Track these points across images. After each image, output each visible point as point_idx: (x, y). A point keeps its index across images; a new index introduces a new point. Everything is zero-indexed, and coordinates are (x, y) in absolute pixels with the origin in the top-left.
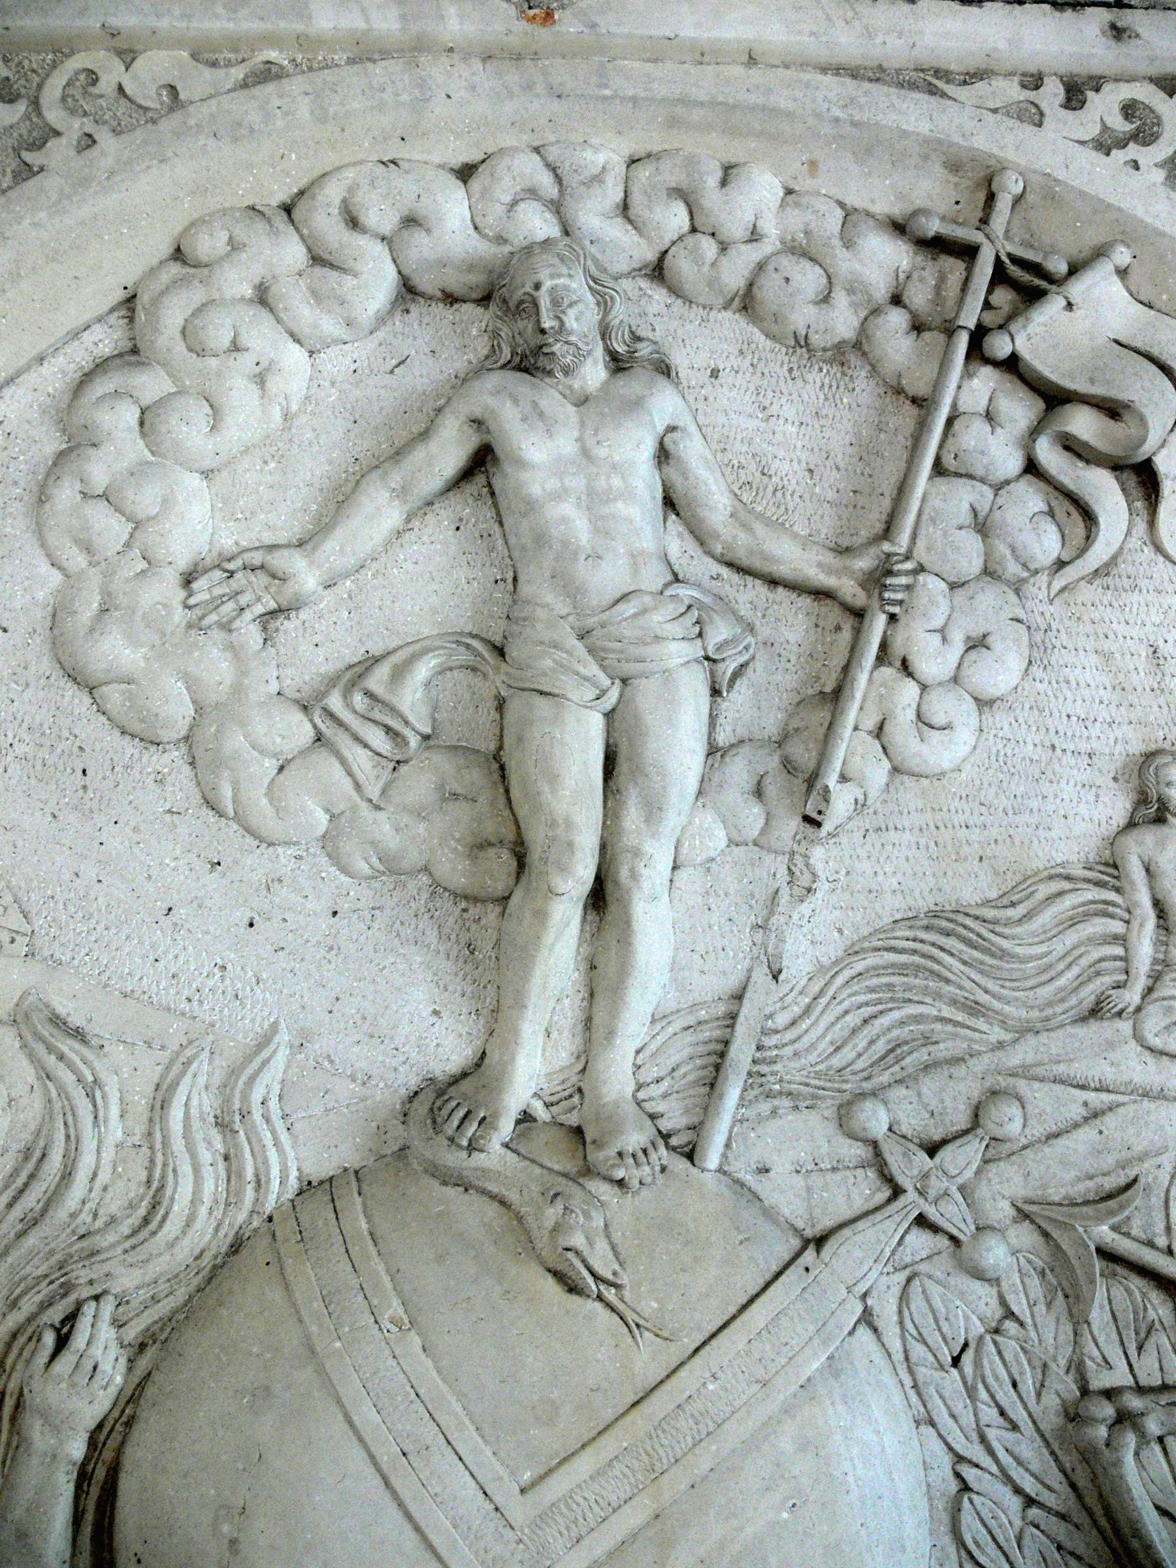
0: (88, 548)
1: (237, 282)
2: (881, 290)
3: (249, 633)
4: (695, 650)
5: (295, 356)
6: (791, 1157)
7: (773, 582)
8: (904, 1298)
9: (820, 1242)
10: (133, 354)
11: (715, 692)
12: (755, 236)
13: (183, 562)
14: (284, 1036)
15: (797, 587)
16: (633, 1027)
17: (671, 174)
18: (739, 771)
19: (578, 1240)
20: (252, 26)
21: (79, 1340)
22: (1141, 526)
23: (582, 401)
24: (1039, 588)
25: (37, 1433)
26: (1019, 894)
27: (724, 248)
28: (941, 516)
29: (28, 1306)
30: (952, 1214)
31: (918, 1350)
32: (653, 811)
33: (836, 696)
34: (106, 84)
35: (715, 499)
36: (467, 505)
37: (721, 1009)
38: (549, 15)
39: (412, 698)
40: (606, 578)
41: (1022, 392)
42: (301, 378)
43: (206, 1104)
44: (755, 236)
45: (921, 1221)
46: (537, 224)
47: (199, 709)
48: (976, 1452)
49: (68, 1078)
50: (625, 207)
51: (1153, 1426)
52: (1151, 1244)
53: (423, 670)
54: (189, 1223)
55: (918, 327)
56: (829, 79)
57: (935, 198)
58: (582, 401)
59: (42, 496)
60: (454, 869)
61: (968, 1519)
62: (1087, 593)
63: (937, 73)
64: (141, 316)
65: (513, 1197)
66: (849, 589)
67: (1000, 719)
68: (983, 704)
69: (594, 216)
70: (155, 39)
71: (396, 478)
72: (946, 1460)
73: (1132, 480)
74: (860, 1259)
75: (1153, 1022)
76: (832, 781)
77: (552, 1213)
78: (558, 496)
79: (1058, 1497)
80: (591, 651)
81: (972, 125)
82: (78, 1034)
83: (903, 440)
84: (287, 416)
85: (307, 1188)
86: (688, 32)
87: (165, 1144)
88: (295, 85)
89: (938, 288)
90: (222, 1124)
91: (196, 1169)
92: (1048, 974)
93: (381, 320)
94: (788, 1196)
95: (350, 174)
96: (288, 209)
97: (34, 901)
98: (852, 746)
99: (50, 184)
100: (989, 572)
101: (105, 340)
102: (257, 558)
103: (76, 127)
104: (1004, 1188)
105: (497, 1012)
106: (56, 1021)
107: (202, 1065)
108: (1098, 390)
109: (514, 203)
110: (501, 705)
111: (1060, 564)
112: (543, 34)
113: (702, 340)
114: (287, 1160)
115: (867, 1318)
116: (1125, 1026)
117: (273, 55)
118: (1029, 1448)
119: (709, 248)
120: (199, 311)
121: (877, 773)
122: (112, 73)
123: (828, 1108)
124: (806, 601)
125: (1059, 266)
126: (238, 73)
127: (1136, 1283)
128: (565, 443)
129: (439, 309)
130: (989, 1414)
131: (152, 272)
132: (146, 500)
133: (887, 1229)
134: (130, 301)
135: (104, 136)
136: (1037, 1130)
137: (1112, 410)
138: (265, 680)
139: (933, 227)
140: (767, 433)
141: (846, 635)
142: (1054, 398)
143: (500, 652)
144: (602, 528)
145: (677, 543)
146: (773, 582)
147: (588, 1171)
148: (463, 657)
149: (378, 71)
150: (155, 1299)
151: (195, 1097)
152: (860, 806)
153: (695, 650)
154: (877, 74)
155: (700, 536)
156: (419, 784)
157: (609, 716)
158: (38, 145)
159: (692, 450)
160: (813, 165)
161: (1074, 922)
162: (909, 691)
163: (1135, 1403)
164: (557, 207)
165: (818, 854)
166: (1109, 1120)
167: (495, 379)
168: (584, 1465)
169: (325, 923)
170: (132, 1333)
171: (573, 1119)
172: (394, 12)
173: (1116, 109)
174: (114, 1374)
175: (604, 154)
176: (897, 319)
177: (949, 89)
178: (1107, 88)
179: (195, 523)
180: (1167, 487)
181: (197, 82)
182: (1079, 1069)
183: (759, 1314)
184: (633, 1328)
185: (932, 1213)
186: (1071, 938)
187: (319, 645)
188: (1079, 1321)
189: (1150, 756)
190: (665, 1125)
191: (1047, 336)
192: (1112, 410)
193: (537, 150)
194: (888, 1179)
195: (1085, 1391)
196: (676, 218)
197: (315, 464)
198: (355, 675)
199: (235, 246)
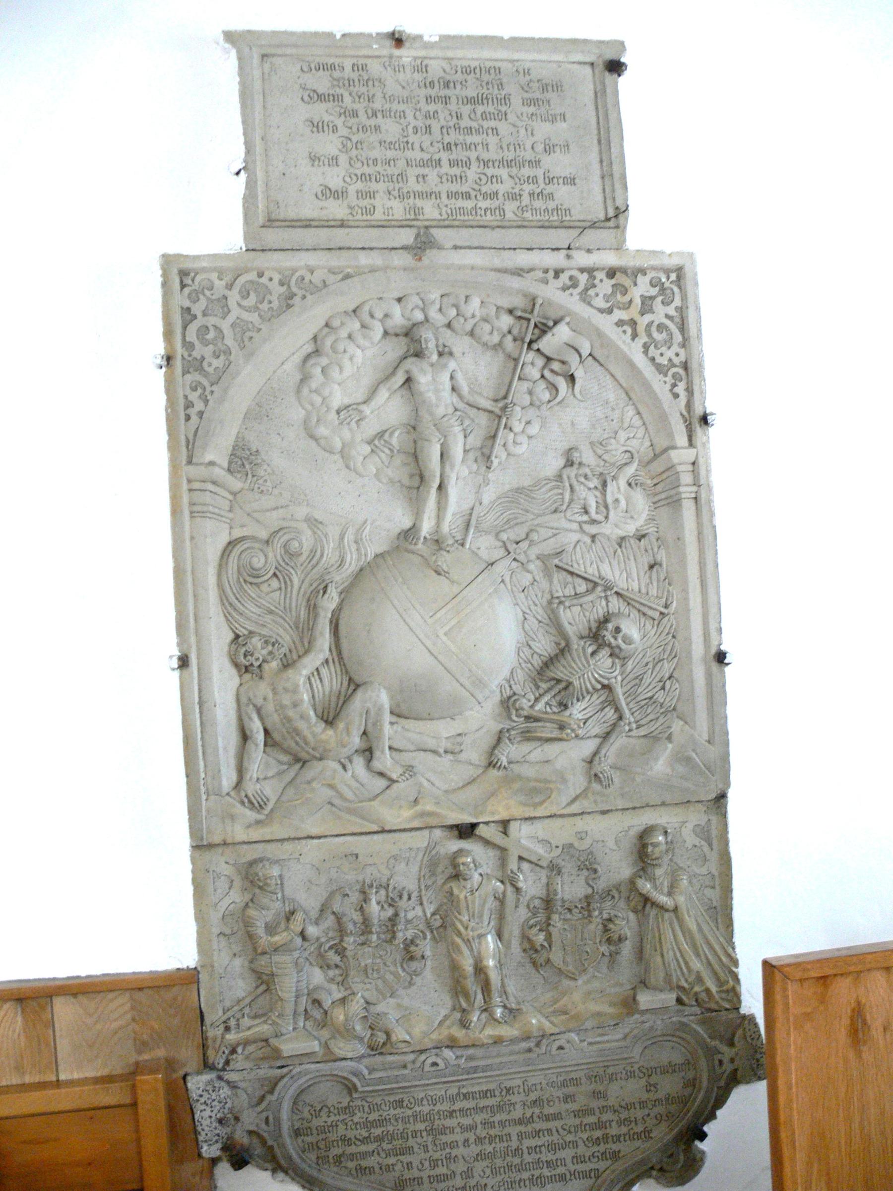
0: (312, 405)
1: (344, 333)
2: (505, 329)
3: (353, 424)
4: (460, 428)
5: (359, 352)
6: (484, 545)
7: (479, 409)
8: (511, 577)
9: (492, 564)
10: (317, 352)
11: (465, 437)
12: (473, 316)
13: (336, 408)
14: (369, 522)
15: (485, 410)
16: (449, 517)
17: (452, 300)
18: (471, 456)
19: (439, 563)
21: (329, 591)
22: (570, 390)
23: (432, 365)
24: (544, 407)
25: (322, 613)
26: (538, 484)
27: (465, 320)
28: (520, 390)
29: (315, 585)
30: (522, 558)
31: (514, 589)
32: (452, 466)
33: (494, 437)
34: (307, 280)
35: (465, 388)
36: (404, 392)
37: (468, 512)
39: (394, 441)
40: (440, 411)
41: (541, 357)
42: (362, 357)
43: (352, 537)
44: (473, 316)
45: (515, 559)
46: (419, 316)
47: (343, 443)
48: (528, 611)
49: (319, 532)
50: (440, 310)
51: (567, 604)
52: (567, 564)
53: (396, 434)
54: (350, 564)
55: (515, 340)
56: (493, 273)
57: (518, 302)
58: (432, 365)
59: (298, 391)
60: (406, 481)
61: (526, 626)
62: (556, 408)
63: (522, 270)
64: (319, 342)
65: (425, 554)
66: (497, 411)
67: (534, 441)
68: (530, 437)
69: (433, 313)
71: (388, 385)
72: (521, 614)
73: (568, 379)
74: (501, 568)
75: (569, 514)
76: (493, 458)
77: (434, 557)
78: (428, 391)
79: (547, 621)
80: (438, 429)
81: (529, 284)
82: (321, 523)
83: (511, 370)
84: (358, 368)
85: (376, 556)
86: (457, 262)
87: (344, 547)
88: (356, 279)
89: (520, 329)
90: (356, 542)
91: (351, 553)
92: (545, 501)
93: (379, 342)
94: (484, 554)
95: (370, 303)
96: (354, 311)
97: (307, 492)
98: (498, 449)
99: (296, 309)
100: (531, 404)
101: (309, 348)
102: (354, 407)
103: (300, 293)
104: (534, 552)
105: (418, 514)
106: (316, 520)
107: (350, 529)
108: (559, 358)
109: (412, 309)
110: (415, 442)
111: (549, 401)
112: (419, 264)
113: (460, 344)
114: (372, 550)
115: (503, 581)
116: (562, 514)
117: (349, 270)
118: (540, 610)
119: (462, 320)
120: (335, 341)
121: (504, 455)
122: (308, 277)
123: (493, 534)
124: (486, 414)
125: (551, 324)
126: (341, 276)
127: (564, 573)
128: (429, 377)
129: (394, 337)
130: (531, 603)
131: (321, 330)
132: (326, 393)
133: (507, 562)
134: (315, 338)
135: (307, 294)
136: (542, 538)
137: (563, 362)
138: (358, 439)
139: (519, 314)
140: (475, 368)
141: (496, 422)
142: (549, 359)
143: (414, 428)
144: (439, 399)
145: (456, 399)
146: (479, 409)
147: (441, 549)
148: (405, 430)
150: (343, 583)
151: (350, 536)
152: (500, 463)
153: (460, 428)
154: (505, 271)
155: (461, 397)
156: (398, 460)
157: (442, 445)
158: (291, 298)
159: (459, 376)
160: (488, 296)
161: (550, 490)
162: (512, 435)
163: (563, 599)
164: (423, 310)
165: (490, 475)
166: (558, 536)
167: (411, 360)
168: (444, 611)
169: (376, 495)
170: (339, 590)
171: (436, 538)
173: (567, 279)
174: (336, 599)
175: (435, 295)
176: (509, 338)
177: (525, 275)
179: (338, 399)
180: (577, 380)
181: (331, 279)
182: (551, 524)
183: (480, 579)
184: (453, 582)
185: (517, 558)
186: (549, 494)
187: (371, 427)
188: (551, 582)
189: (570, 449)
190: (457, 539)
191: (547, 344)
192: (563, 362)
193: (418, 294)
194: (507, 550)
195: (552, 597)
196: (453, 312)
197: (367, 381)
198: (381, 435)
199: (343, 324)
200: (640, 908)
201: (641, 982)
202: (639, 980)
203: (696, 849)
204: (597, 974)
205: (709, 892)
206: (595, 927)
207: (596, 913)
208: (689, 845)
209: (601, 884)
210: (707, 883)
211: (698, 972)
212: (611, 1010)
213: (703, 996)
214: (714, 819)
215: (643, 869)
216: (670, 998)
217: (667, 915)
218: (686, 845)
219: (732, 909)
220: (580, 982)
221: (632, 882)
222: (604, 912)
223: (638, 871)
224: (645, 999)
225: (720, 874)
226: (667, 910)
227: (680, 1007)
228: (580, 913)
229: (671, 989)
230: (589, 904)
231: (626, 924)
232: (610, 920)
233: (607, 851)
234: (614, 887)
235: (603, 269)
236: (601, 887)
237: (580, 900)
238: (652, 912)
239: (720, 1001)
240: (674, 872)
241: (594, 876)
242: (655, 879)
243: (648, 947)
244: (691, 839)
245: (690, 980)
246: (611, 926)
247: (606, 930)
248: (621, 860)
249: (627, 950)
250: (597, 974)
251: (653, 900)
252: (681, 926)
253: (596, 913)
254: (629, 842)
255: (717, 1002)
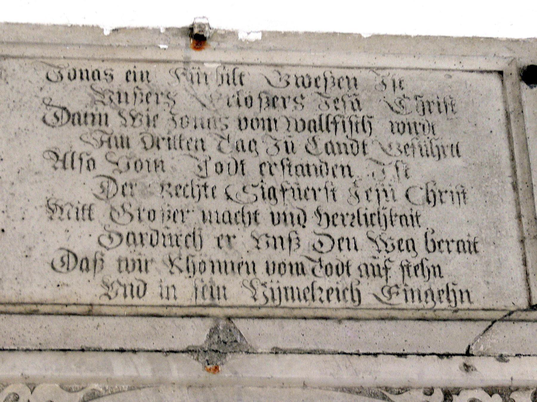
20: (89, 375)
38: (216, 368)
56: (339, 394)
63: (387, 389)
70: (44, 380)
86: (278, 375)
112: (214, 377)
117: (96, 386)
149: (141, 393)
172: (149, 368)
177: (392, 397)
178: (462, 393)
235: (527, 389)
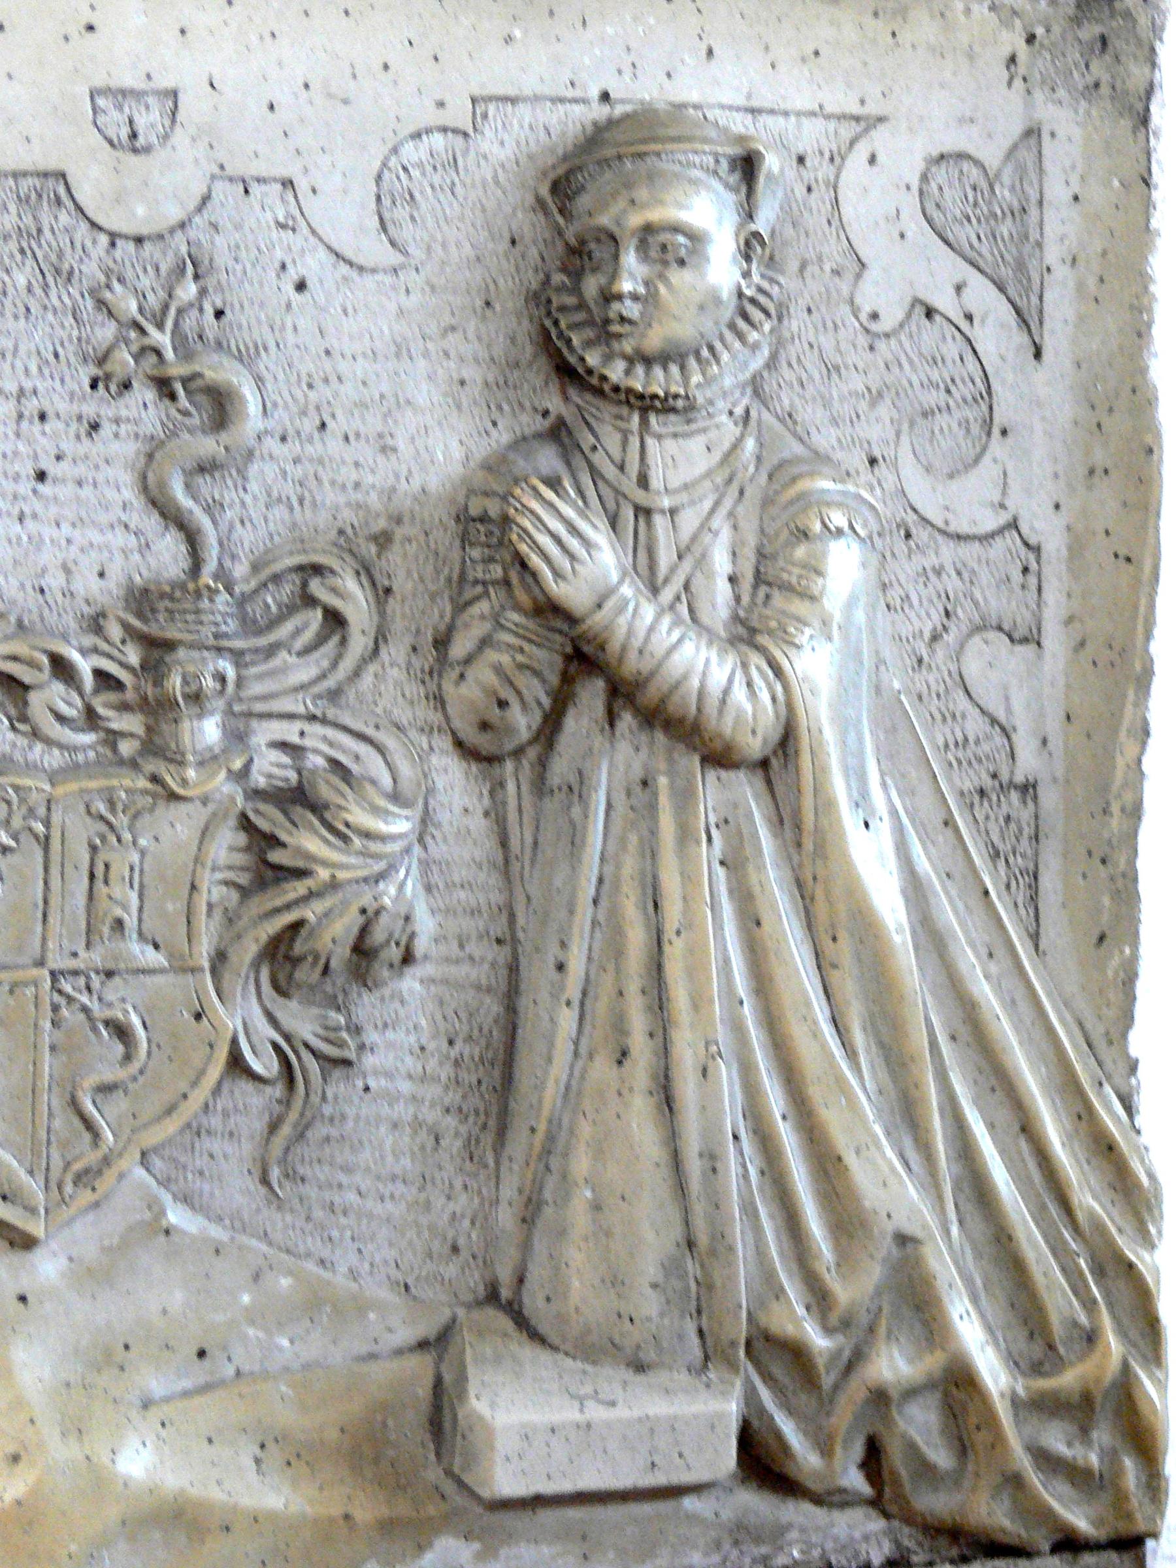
200: (523, 723)
201: (492, 1296)
202: (475, 1281)
203: (929, 334)
204: (176, 1216)
205: (991, 666)
206: (187, 841)
207: (210, 730)
208: (881, 294)
209: (252, 521)
210: (997, 603)
211: (902, 1239)
212: (273, 1496)
213: (920, 1426)
214: (1069, 129)
215: (558, 433)
216: (694, 1418)
217: (713, 793)
218: (870, 295)
219: (1135, 812)
220: (47, 1266)
221: (485, 534)
222: (264, 733)
223: (521, 443)
224: (529, 1420)
225: (1076, 548)
226: (719, 757)
227: (754, 1502)
228: (91, 718)
229: (712, 1354)
230: (157, 650)
231: (412, 841)
232: (298, 798)
233: (315, 264)
234: (344, 540)
236: (248, 539)
237: (96, 624)
238: (608, 760)
239: (1034, 1478)
240: (781, 473)
241: (209, 446)
242: (644, 512)
243: (555, 1026)
244: (903, 265)
245: (843, 1293)
246: (309, 841)
247: (267, 865)
248: (400, 350)
249: (404, 1034)
250: (176, 1216)
251: (632, 665)
252: (804, 891)
253: (210, 730)
254: (470, 220)
255: (1016, 1481)
